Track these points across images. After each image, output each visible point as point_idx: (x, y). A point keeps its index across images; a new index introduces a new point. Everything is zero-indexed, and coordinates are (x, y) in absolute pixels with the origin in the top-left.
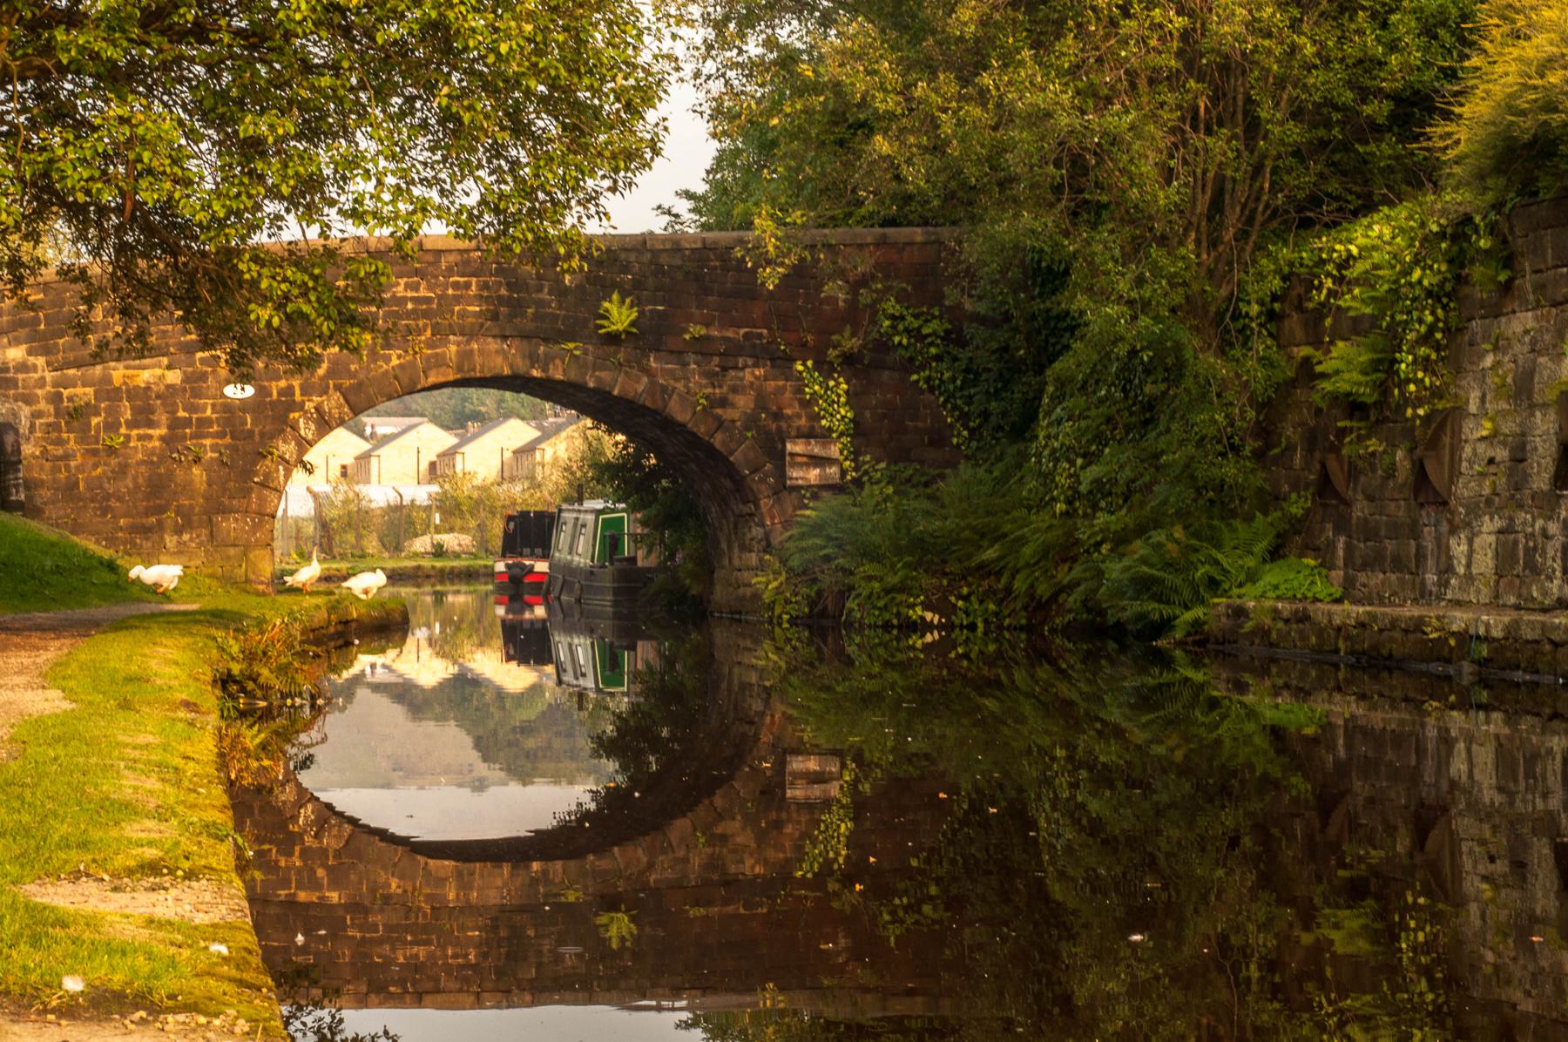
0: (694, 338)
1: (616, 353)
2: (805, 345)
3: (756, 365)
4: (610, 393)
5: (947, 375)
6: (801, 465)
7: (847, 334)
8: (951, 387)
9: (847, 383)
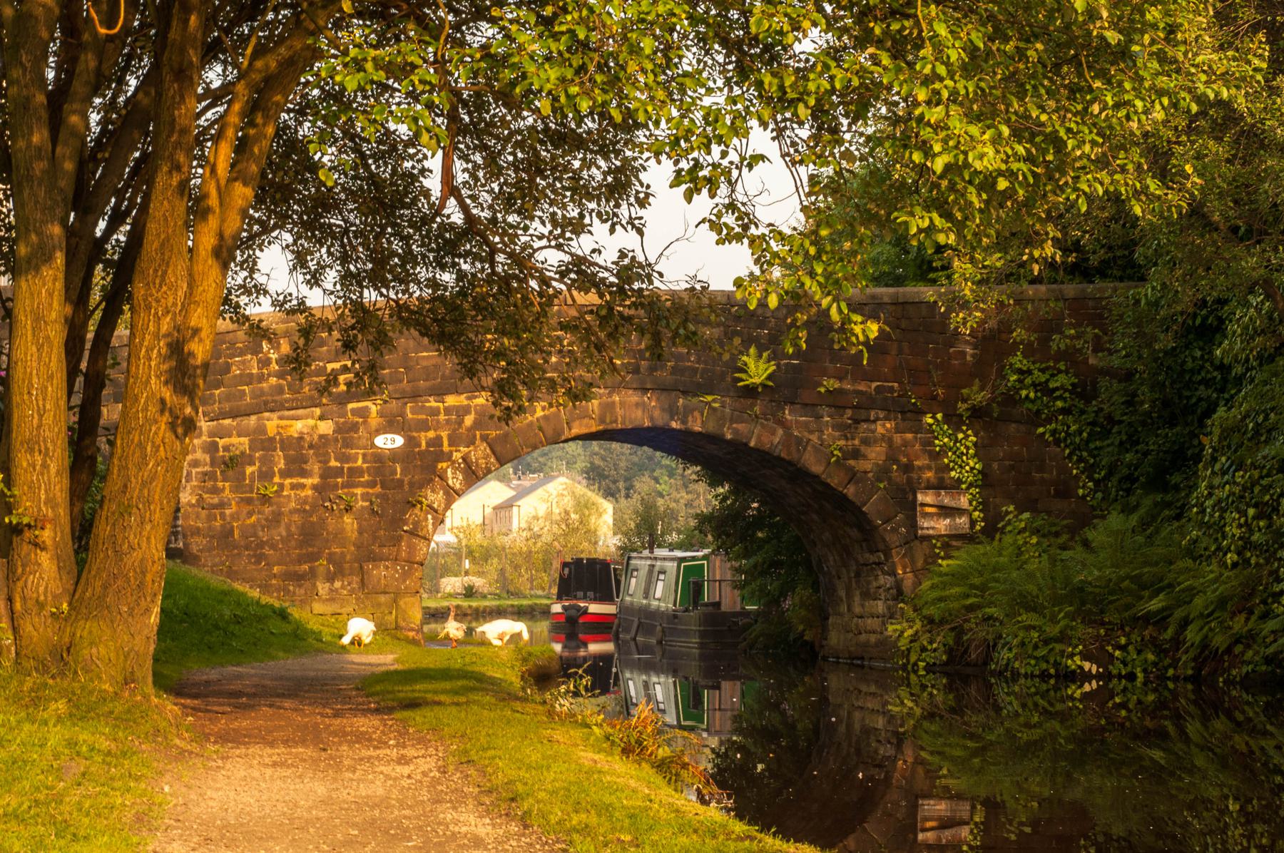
0: (828, 391)
1: (753, 405)
2: (934, 398)
3: (887, 419)
4: (746, 445)
5: (1073, 428)
6: (930, 515)
7: (975, 388)
8: (1077, 440)
9: (975, 435)
